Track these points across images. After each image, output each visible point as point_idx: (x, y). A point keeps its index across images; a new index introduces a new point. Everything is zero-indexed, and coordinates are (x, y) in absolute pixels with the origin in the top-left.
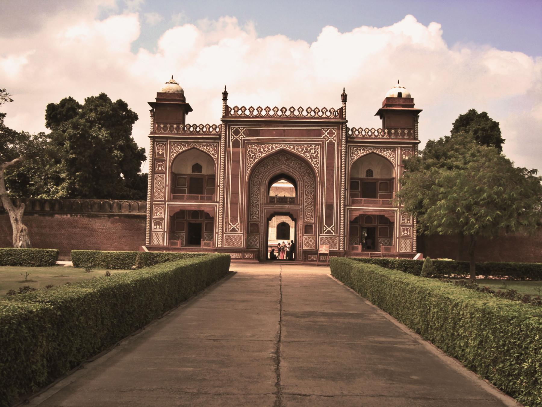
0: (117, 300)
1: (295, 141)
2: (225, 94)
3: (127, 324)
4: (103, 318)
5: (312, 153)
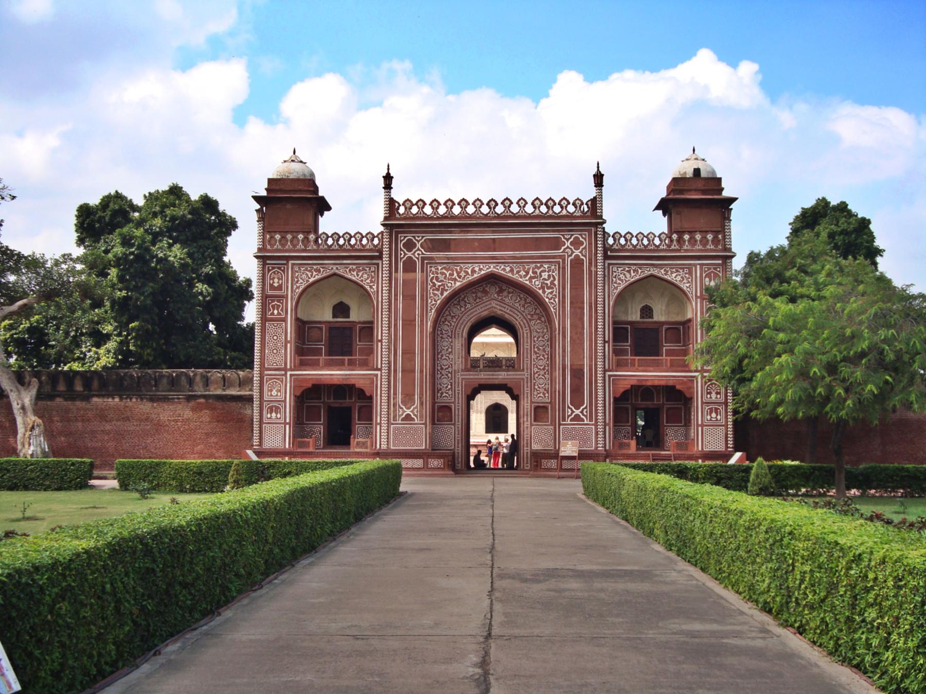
0: (154, 561)
2: (388, 179)
3: (181, 607)
4: (118, 602)
5: (544, 279)
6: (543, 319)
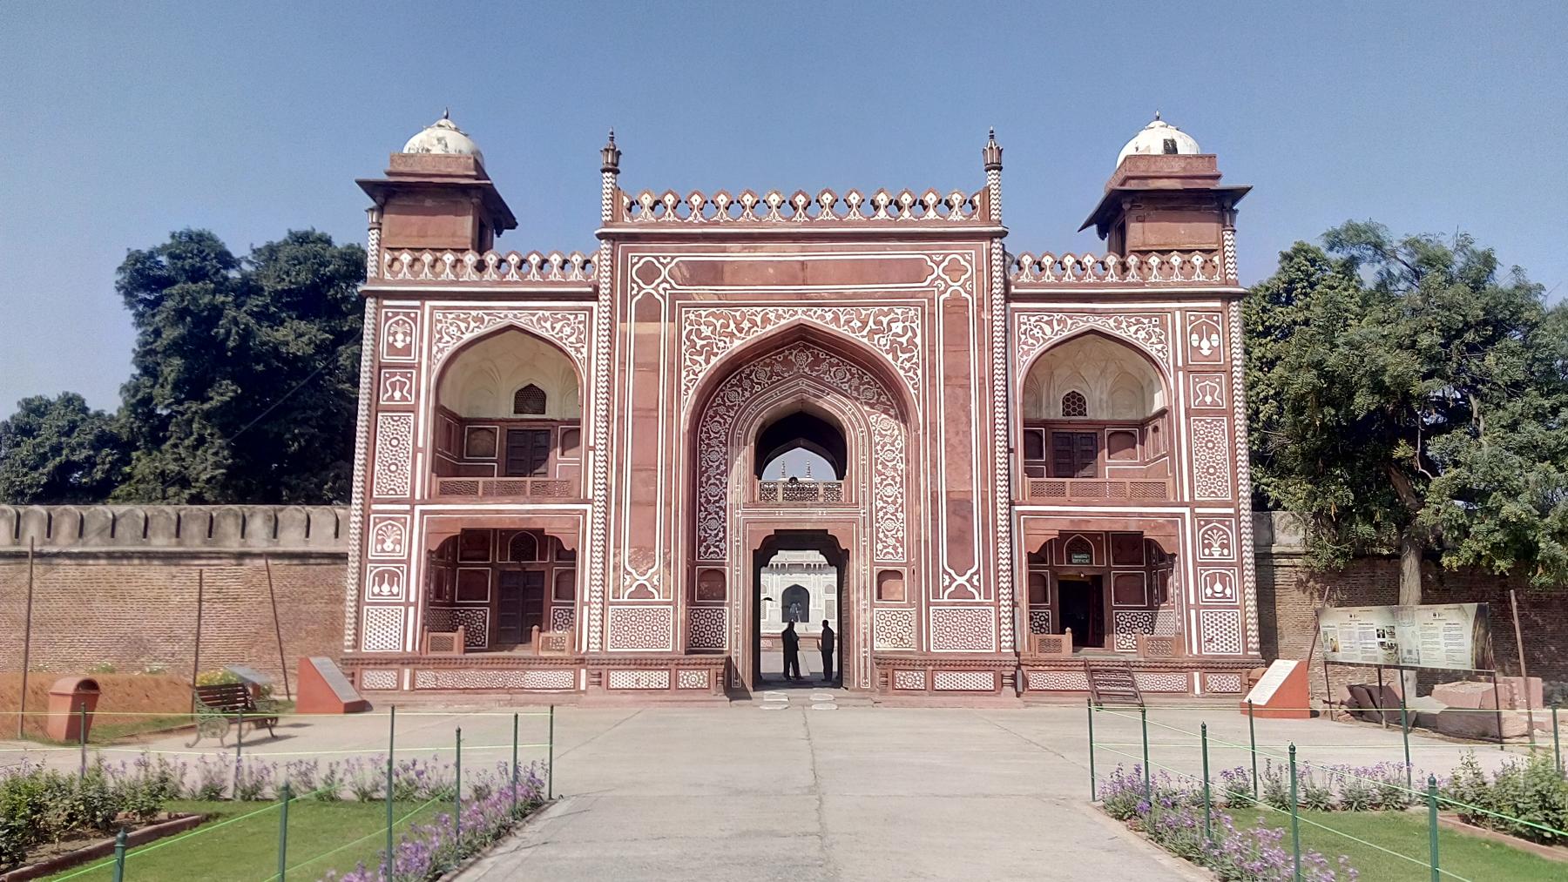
1: (842, 296)
6: (892, 412)
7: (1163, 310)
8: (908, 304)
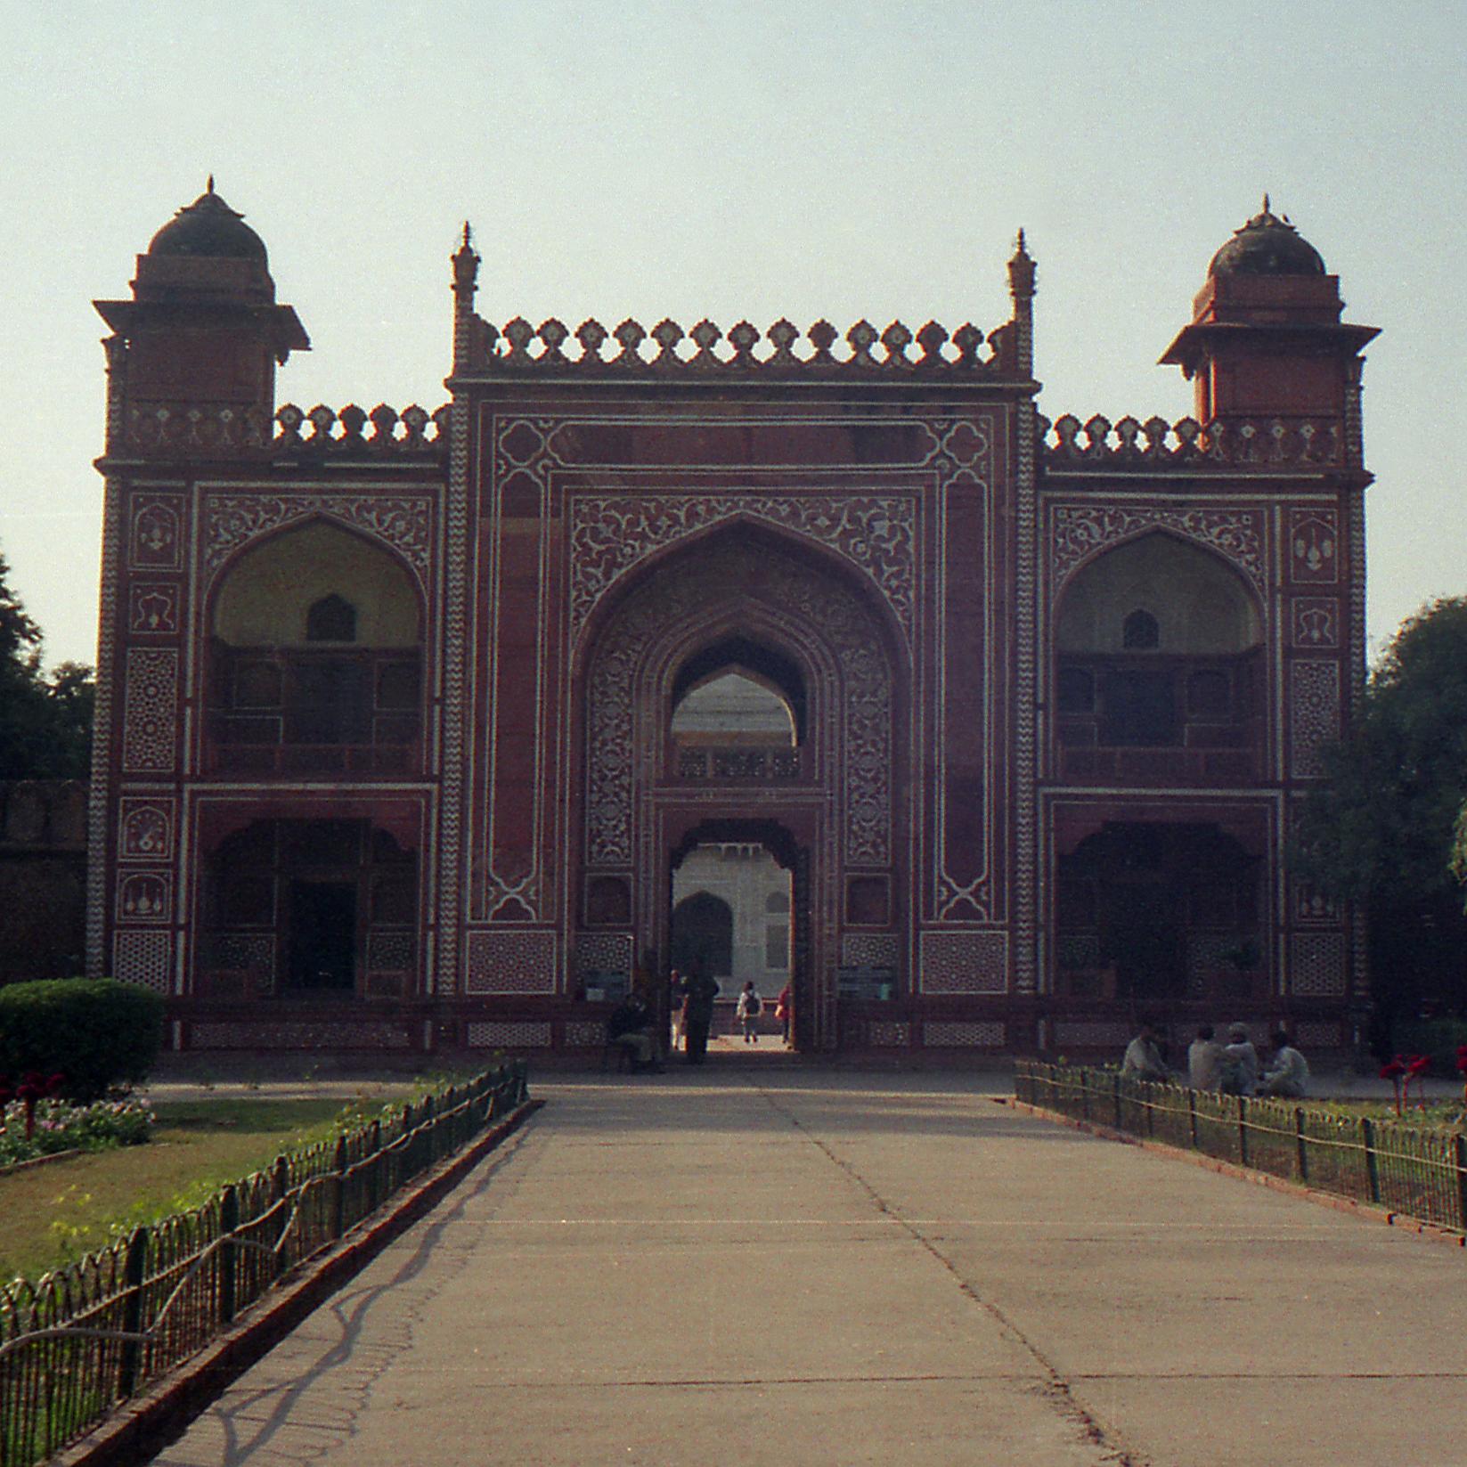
5: (880, 537)
7: (1258, 502)
8: (898, 493)
